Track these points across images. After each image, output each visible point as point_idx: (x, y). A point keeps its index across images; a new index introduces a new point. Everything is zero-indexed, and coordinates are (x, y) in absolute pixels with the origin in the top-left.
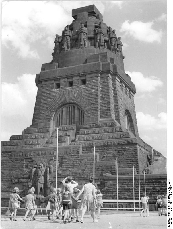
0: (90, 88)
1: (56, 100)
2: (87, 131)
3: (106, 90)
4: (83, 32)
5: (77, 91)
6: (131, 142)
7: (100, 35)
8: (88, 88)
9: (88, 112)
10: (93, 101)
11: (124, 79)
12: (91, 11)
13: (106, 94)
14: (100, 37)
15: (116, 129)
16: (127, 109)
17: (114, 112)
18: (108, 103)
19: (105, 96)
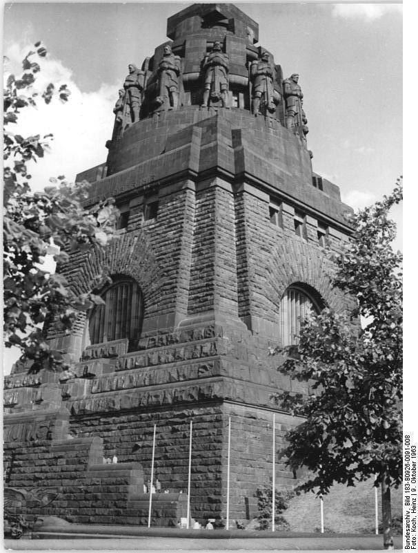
0: (164, 225)
1: (89, 272)
2: (132, 360)
3: (207, 226)
4: (165, 69)
5: (136, 239)
6: (206, 392)
7: (213, 70)
8: (160, 226)
9: (154, 298)
10: (168, 264)
11: (285, 191)
13: (205, 240)
14: (214, 76)
15: (202, 348)
16: (295, 280)
17: (236, 294)
18: (208, 267)
19: (203, 245)
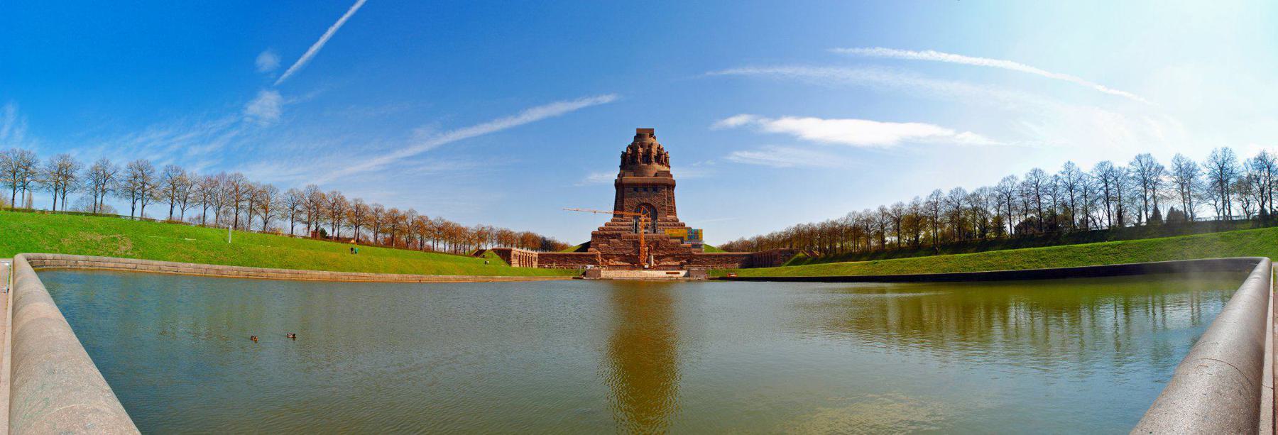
12: (651, 133)
